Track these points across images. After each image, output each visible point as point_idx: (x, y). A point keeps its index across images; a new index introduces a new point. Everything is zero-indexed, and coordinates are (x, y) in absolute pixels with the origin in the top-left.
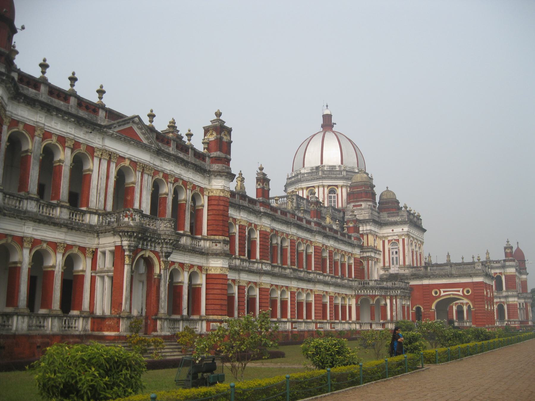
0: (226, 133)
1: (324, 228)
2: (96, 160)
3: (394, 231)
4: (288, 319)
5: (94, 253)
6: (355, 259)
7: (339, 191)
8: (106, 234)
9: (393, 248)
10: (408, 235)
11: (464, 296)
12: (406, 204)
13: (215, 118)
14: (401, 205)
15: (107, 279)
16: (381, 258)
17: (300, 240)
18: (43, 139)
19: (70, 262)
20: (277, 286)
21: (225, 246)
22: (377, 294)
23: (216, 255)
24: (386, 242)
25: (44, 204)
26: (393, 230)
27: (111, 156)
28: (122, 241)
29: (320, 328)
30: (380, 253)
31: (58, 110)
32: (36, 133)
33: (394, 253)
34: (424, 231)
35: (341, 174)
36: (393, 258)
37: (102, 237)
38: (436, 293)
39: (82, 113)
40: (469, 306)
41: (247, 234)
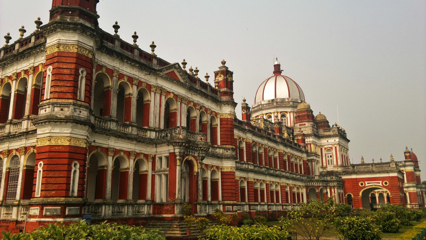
0: (230, 75)
1: (284, 140)
2: (153, 94)
3: (329, 142)
4: (265, 203)
5: (154, 158)
6: (304, 161)
7: (288, 115)
8: (162, 144)
9: (329, 154)
10: (339, 144)
11: (384, 186)
12: (336, 123)
13: (222, 65)
14: (331, 124)
15: (163, 177)
16: (320, 160)
17: (270, 149)
18: (119, 79)
19: (137, 165)
20: (257, 180)
21: (233, 152)
22: (320, 185)
23: (228, 158)
24: (323, 149)
25: (121, 124)
26: (328, 141)
27: (162, 91)
28: (174, 149)
29: (285, 209)
30: (319, 157)
31: (128, 58)
32: (114, 75)
33: (329, 156)
34: (349, 141)
35: (289, 104)
36: (328, 160)
37: (159, 147)
38: (362, 184)
39: (142, 61)
40: (388, 194)
41: (238, 144)
